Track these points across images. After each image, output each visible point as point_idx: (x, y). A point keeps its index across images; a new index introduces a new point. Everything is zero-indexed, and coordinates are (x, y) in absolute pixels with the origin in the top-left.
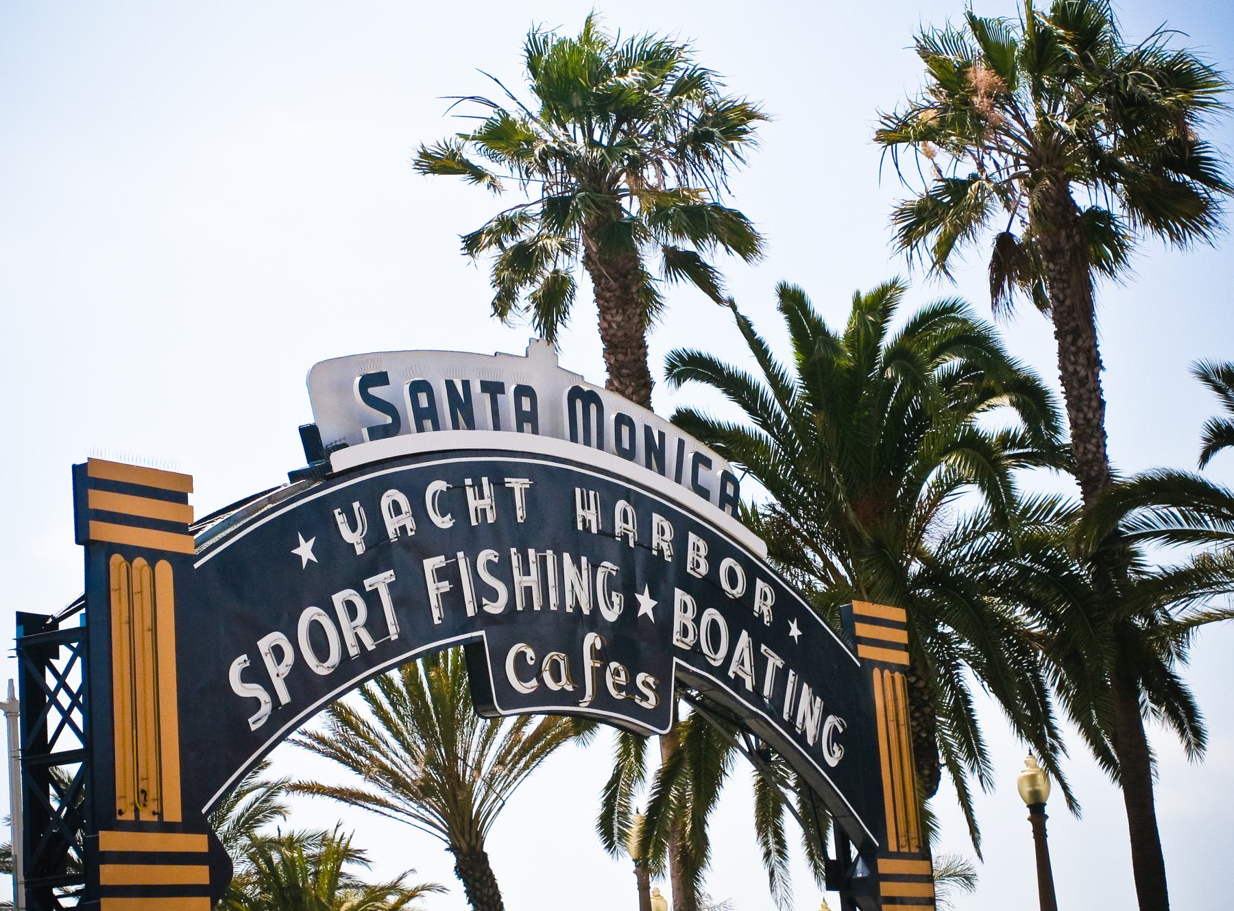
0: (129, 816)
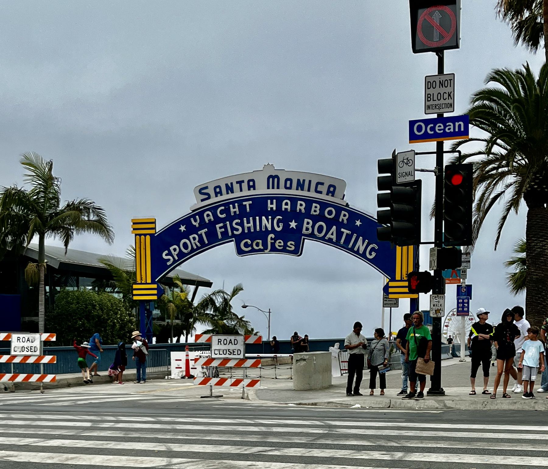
0: (139, 282)
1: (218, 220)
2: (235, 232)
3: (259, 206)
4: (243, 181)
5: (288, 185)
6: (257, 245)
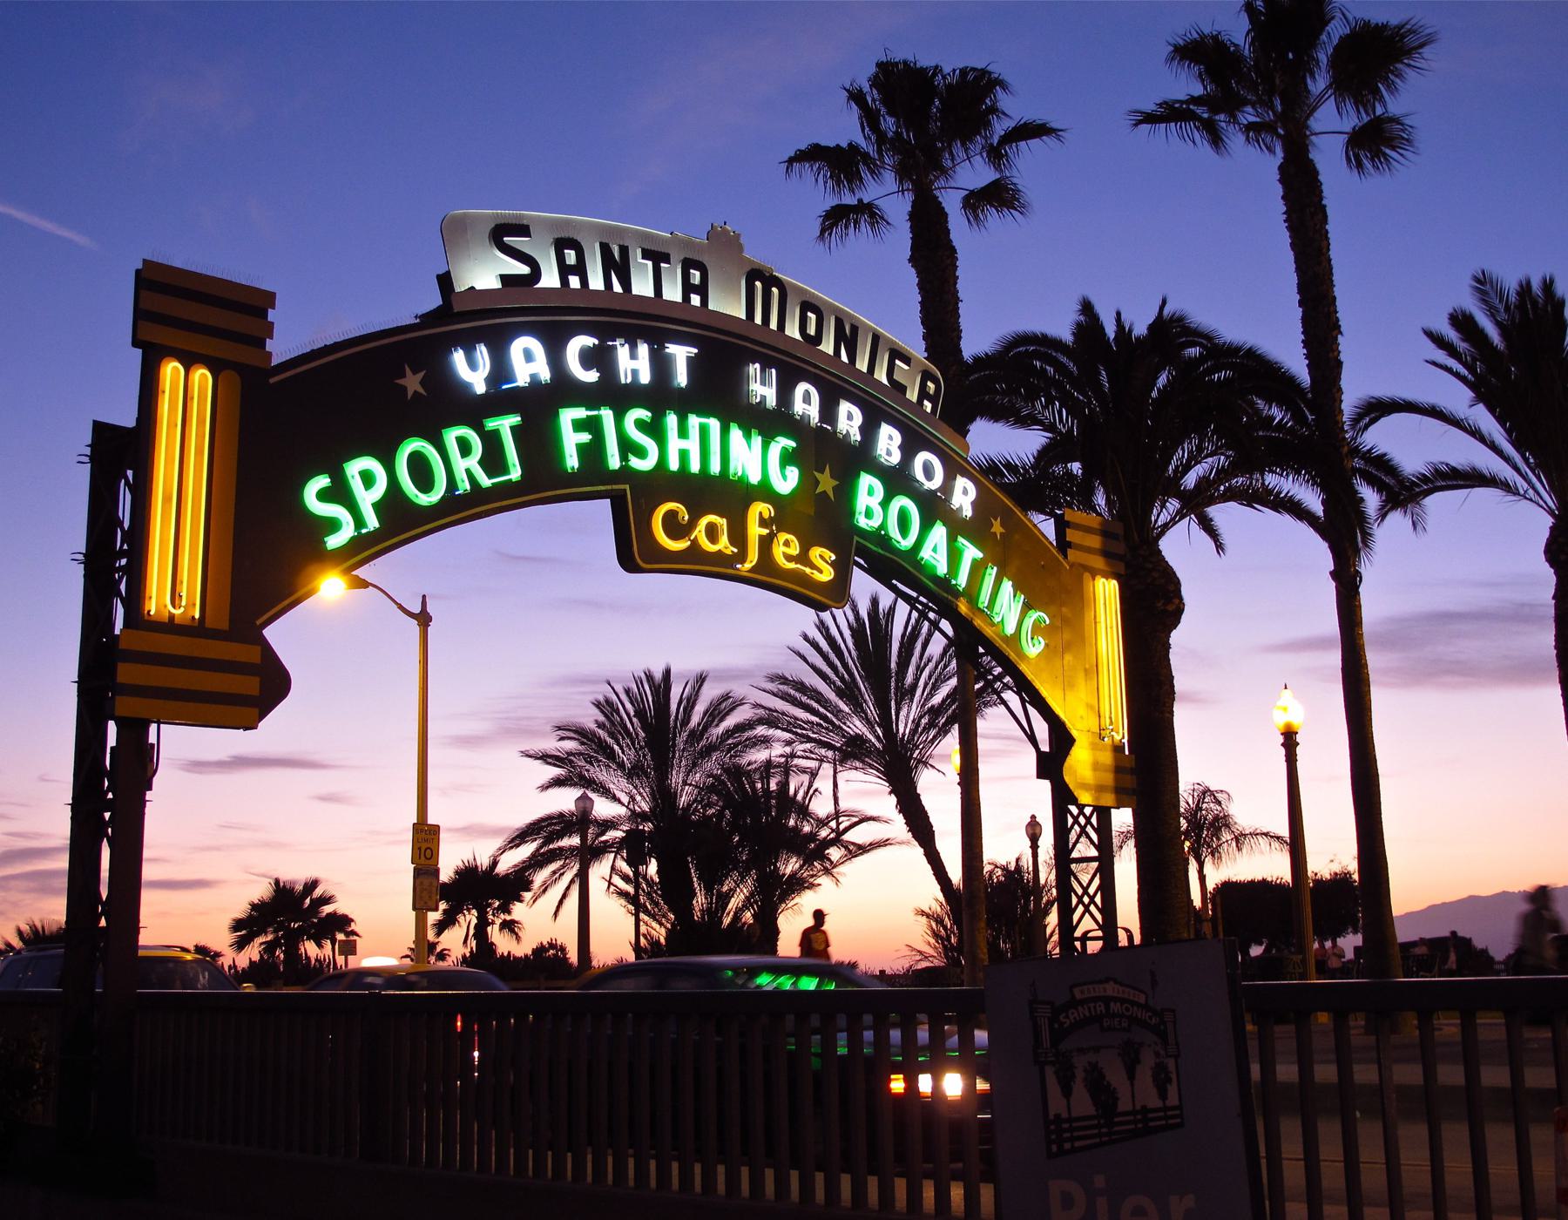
2: (636, 463)
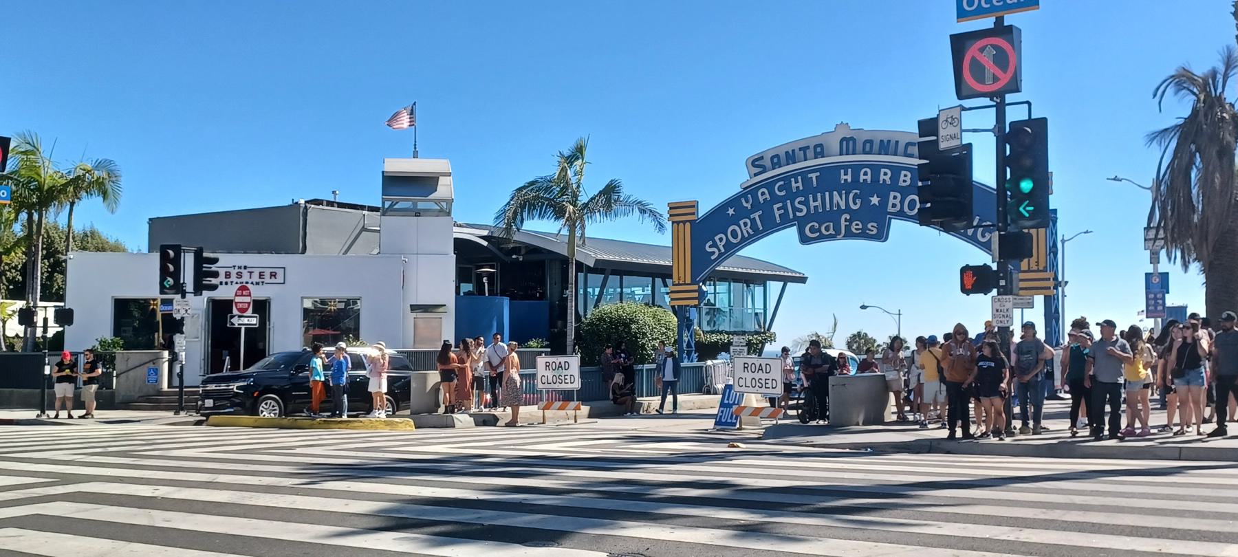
1: (775, 199)
2: (798, 214)
3: (829, 178)
4: (808, 147)
5: (868, 148)
6: (827, 229)
